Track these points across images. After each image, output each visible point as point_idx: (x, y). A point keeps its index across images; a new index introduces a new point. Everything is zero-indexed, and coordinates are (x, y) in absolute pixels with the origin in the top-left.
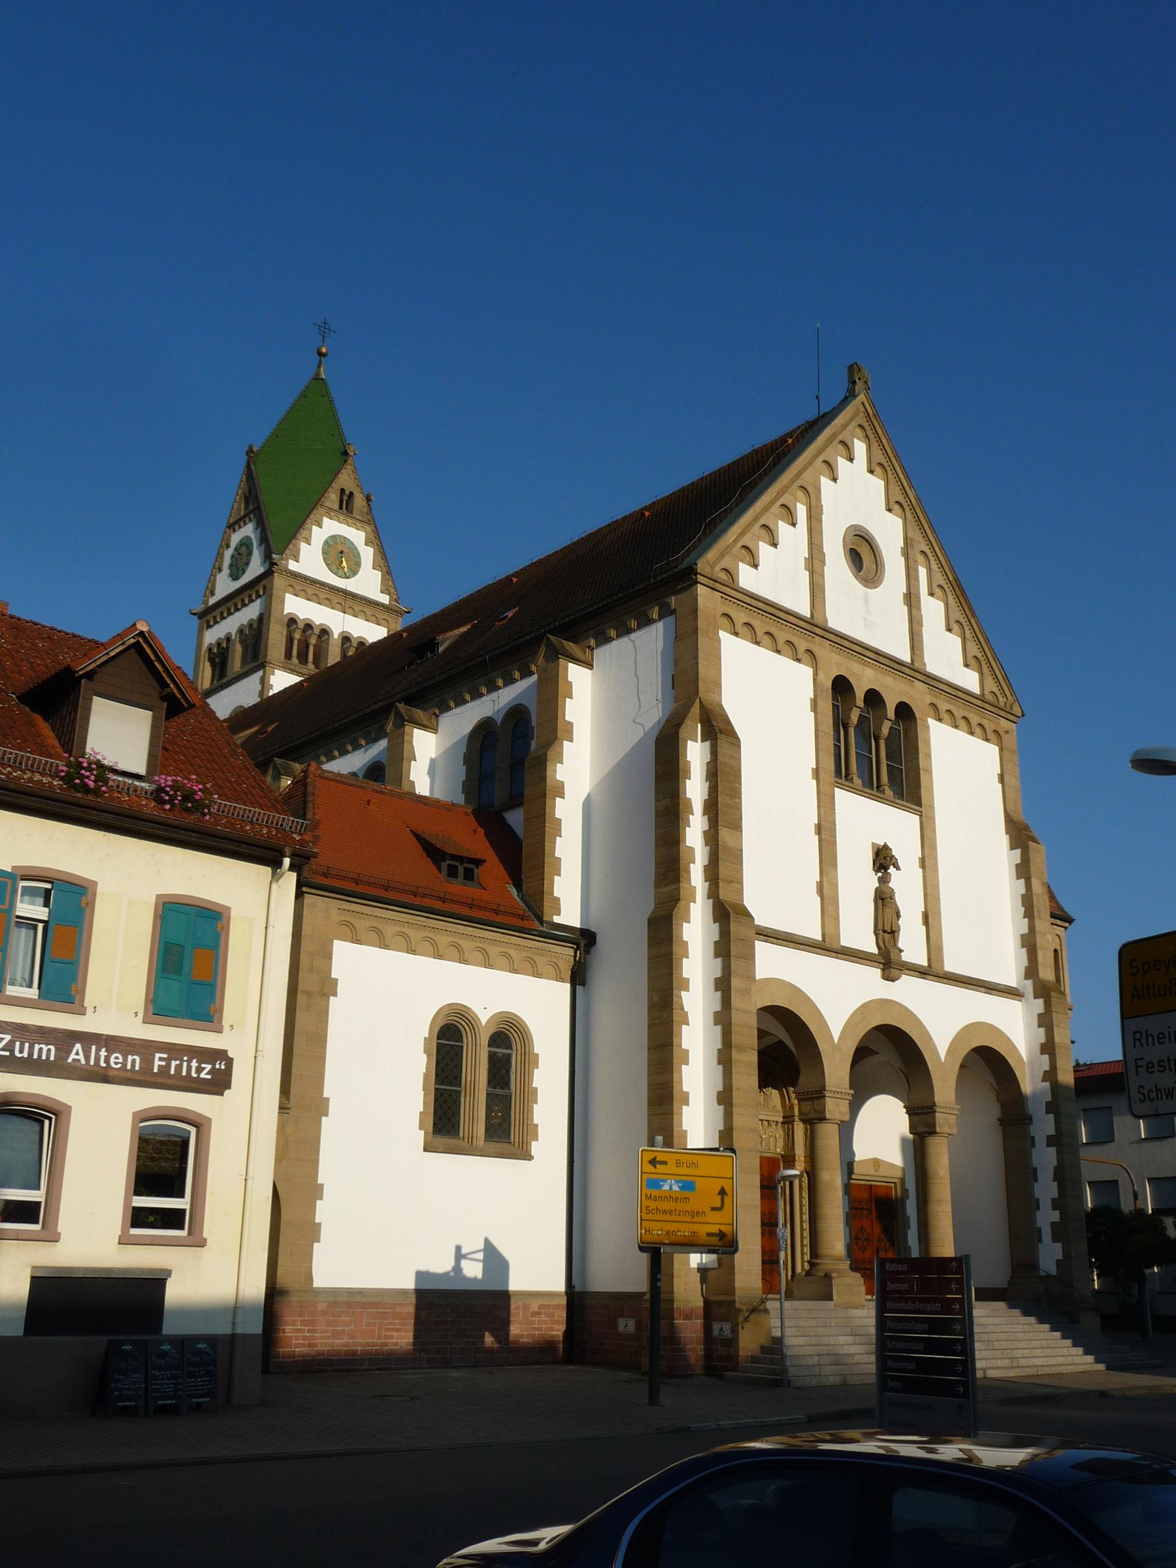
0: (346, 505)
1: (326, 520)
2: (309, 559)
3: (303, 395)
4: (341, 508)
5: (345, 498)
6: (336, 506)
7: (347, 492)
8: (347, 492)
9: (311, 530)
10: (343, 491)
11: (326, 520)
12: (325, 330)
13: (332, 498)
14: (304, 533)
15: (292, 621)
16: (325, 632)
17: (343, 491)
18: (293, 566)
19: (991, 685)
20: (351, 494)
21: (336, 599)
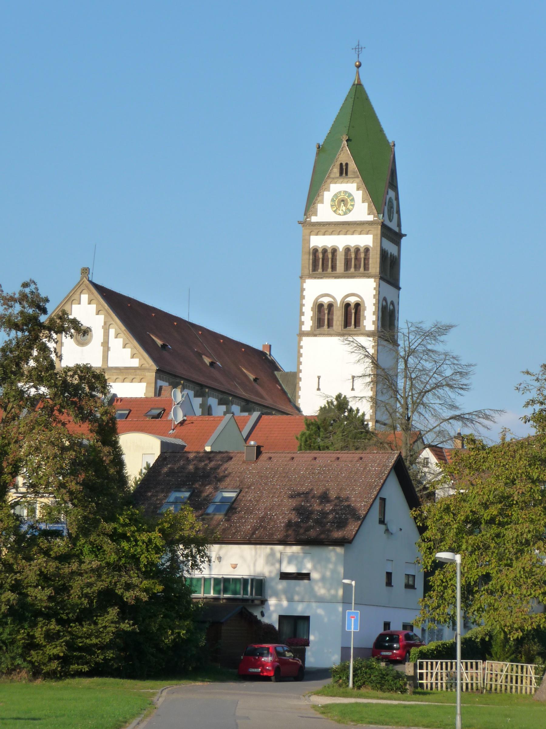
0: (344, 171)
1: (332, 186)
2: (324, 212)
3: (346, 100)
4: (341, 174)
5: (344, 167)
6: (338, 175)
7: (344, 164)
8: (344, 164)
9: (323, 195)
10: (341, 164)
11: (332, 186)
12: (359, 49)
13: (336, 170)
14: (319, 199)
15: (315, 251)
16: (334, 251)
17: (341, 164)
18: (314, 219)
19: (143, 362)
20: (347, 164)
21: (338, 229)
